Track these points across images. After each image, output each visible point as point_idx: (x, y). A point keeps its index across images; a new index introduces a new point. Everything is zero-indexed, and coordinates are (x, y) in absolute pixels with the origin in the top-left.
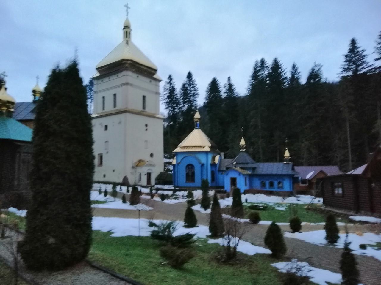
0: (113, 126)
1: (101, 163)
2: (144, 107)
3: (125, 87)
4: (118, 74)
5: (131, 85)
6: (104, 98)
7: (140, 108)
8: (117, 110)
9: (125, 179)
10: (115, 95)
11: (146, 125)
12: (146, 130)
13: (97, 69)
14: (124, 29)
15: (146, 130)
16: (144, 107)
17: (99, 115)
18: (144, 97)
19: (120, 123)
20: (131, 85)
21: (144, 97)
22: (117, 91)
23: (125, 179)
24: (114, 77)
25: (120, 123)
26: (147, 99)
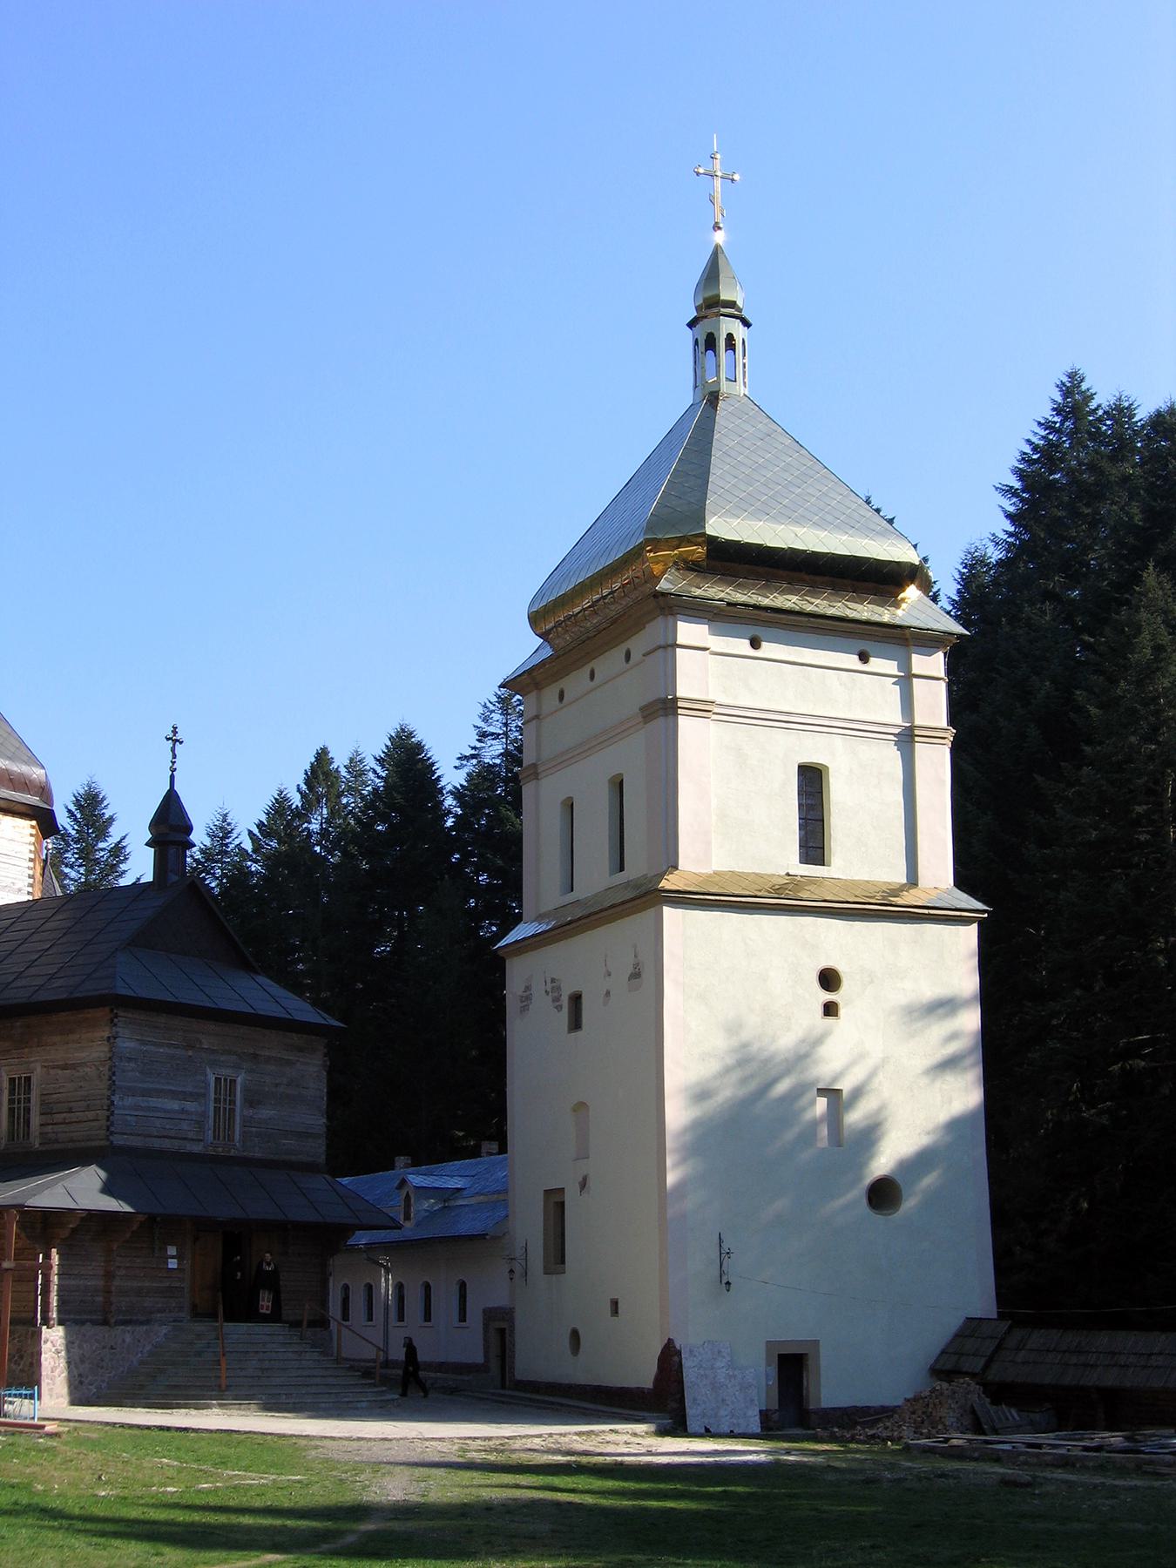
0: (608, 993)
1: (557, 1256)
2: (813, 846)
3: (659, 723)
4: (629, 644)
5: (703, 709)
6: (569, 806)
7: (779, 855)
8: (627, 885)
9: (670, 1358)
10: (618, 785)
11: (829, 979)
12: (830, 1009)
13: (535, 619)
14: (691, 325)
15: (830, 1009)
16: (813, 846)
17: (544, 927)
18: (812, 780)
19: (636, 975)
20: (703, 709)
21: (812, 780)
22: (626, 757)
23: (670, 1358)
24: (609, 663)
25: (636, 975)
26: (838, 792)
